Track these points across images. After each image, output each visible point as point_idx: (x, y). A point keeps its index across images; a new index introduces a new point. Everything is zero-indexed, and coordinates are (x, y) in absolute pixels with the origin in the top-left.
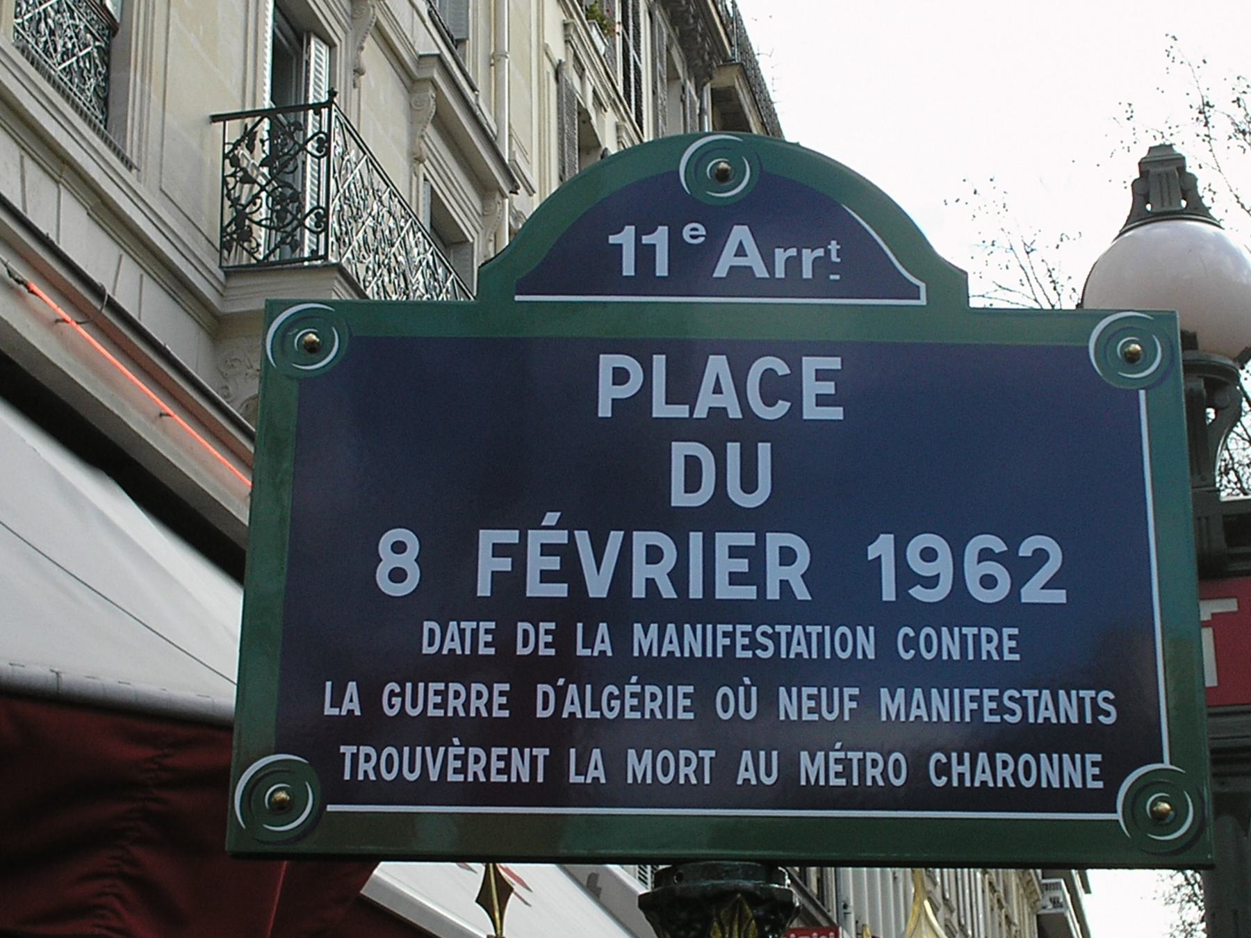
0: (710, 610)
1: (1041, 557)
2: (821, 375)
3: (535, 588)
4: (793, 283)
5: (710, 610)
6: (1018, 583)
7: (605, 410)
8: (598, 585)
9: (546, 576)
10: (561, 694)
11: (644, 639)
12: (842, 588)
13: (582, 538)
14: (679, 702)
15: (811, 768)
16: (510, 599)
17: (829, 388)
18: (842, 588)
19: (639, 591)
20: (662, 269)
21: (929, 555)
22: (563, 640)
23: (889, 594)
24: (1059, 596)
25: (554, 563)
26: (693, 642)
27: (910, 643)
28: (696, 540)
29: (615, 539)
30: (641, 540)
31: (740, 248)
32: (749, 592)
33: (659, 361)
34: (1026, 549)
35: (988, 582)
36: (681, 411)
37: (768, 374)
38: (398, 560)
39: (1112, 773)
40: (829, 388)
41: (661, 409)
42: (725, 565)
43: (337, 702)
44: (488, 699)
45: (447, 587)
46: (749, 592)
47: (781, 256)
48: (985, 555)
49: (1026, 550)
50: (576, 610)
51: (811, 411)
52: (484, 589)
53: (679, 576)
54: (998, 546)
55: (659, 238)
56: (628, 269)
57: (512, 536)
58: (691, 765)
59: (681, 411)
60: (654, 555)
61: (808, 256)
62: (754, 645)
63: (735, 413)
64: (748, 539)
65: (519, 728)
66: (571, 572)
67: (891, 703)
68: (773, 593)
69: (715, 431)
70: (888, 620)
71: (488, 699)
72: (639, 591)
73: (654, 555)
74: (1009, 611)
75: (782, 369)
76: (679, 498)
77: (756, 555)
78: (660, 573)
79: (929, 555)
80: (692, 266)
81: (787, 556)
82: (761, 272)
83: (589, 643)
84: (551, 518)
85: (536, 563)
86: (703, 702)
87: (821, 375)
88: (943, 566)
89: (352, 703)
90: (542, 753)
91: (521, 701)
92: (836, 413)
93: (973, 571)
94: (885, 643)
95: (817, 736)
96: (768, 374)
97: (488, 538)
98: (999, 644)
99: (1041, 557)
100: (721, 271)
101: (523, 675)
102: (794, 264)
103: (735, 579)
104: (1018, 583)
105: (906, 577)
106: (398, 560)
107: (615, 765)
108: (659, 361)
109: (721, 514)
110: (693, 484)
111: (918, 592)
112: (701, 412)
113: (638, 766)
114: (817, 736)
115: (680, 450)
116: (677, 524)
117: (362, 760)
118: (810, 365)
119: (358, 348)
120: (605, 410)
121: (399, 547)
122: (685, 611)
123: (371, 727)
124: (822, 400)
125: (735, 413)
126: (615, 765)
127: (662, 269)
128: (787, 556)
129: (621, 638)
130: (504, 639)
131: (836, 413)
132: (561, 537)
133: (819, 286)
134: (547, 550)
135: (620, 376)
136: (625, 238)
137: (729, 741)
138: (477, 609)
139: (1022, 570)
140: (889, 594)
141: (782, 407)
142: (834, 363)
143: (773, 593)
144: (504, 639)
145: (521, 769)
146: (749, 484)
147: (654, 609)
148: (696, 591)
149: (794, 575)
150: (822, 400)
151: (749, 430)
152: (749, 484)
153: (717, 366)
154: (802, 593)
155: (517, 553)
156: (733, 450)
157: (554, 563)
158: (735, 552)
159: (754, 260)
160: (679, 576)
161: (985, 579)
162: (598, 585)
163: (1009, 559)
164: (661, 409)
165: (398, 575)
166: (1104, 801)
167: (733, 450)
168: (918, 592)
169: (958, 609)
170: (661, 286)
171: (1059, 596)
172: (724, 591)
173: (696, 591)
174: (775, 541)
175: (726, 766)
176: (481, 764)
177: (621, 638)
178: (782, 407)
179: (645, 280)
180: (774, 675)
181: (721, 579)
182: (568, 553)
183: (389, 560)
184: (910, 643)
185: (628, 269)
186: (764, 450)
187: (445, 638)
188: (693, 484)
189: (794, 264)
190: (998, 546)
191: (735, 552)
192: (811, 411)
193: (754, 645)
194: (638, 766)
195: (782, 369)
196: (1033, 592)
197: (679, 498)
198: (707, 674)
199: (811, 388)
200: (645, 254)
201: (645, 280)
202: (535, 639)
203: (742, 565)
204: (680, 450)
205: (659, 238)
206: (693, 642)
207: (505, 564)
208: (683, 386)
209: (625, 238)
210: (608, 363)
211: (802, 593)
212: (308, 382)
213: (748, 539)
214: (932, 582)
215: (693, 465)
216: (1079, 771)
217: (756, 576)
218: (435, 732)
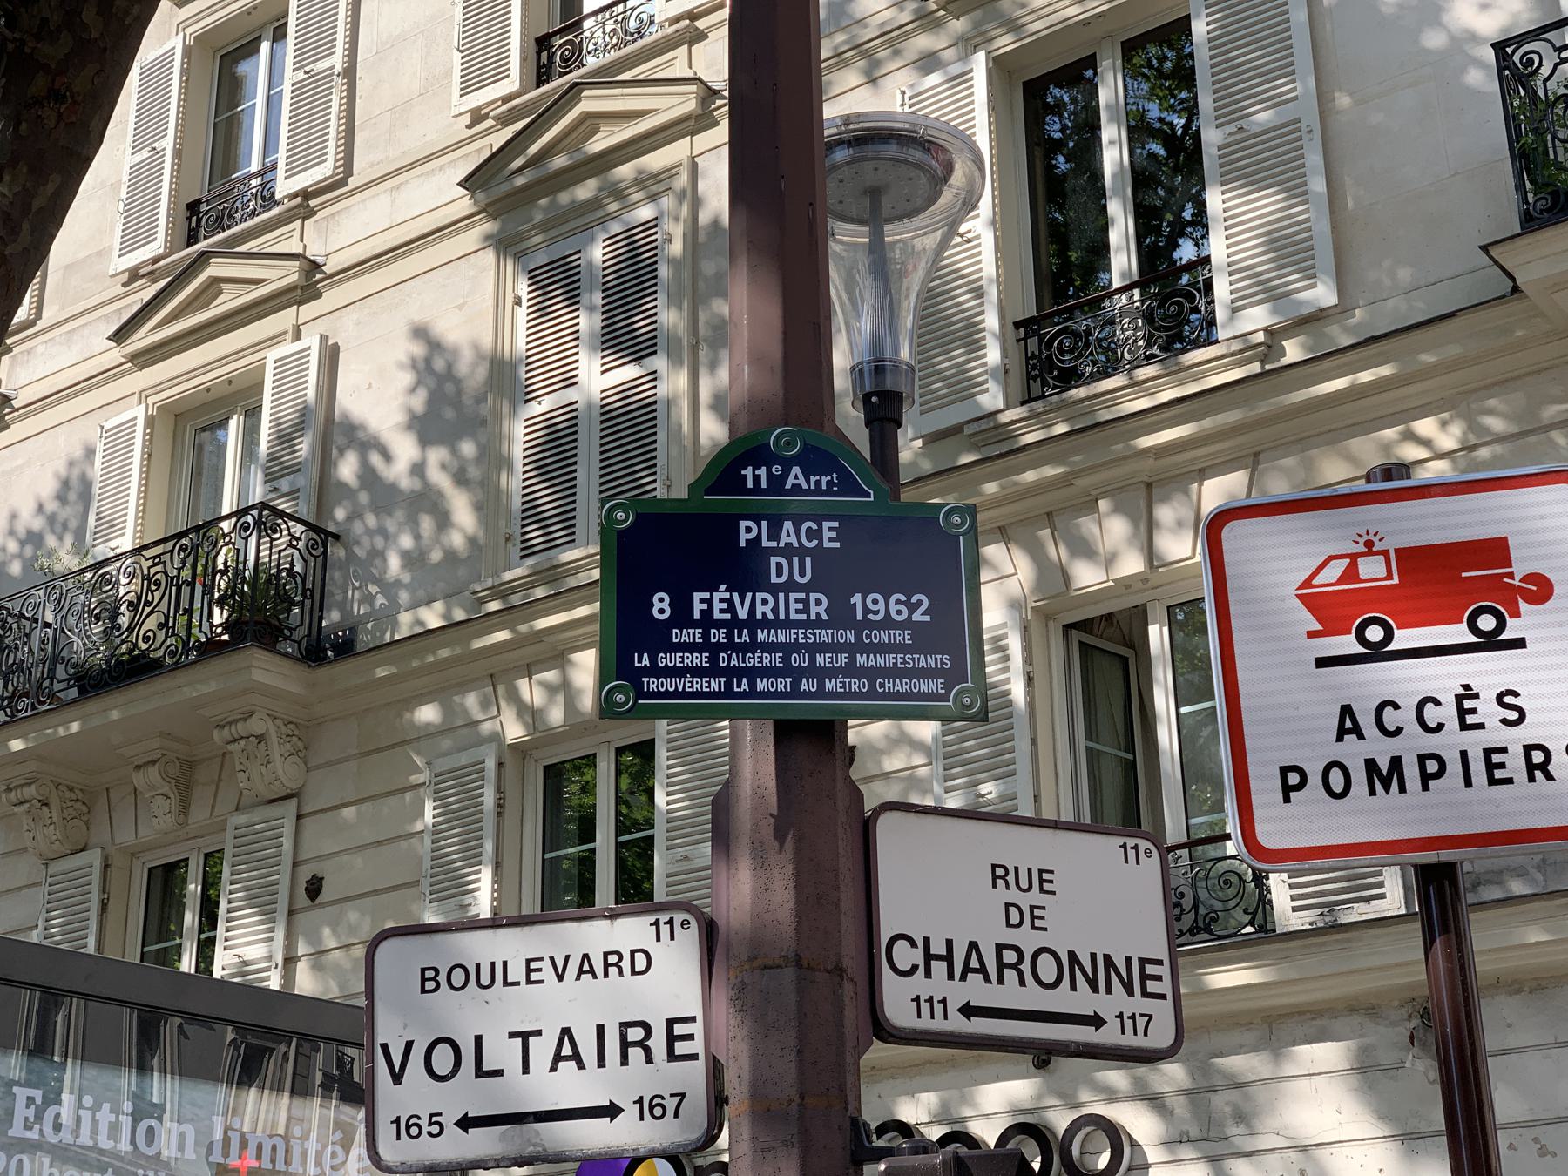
0: (788, 624)
1: (920, 602)
2: (831, 529)
3: (717, 616)
4: (818, 491)
5: (788, 624)
6: (911, 613)
7: (742, 544)
8: (743, 614)
9: (722, 611)
10: (730, 657)
11: (762, 635)
12: (841, 616)
13: (736, 595)
14: (777, 660)
15: (830, 685)
16: (707, 620)
17: (834, 534)
18: (841, 616)
19: (759, 617)
20: (764, 485)
21: (875, 602)
22: (729, 636)
23: (860, 617)
24: (927, 618)
25: (724, 606)
26: (782, 636)
27: (868, 636)
28: (781, 596)
29: (749, 596)
30: (760, 596)
31: (796, 476)
32: (804, 617)
33: (764, 523)
34: (914, 599)
35: (899, 612)
36: (774, 544)
37: (809, 528)
38: (661, 605)
39: (948, 687)
40: (834, 534)
41: (765, 543)
42: (793, 606)
43: (640, 661)
44: (701, 660)
45: (682, 615)
46: (804, 617)
47: (813, 479)
48: (898, 602)
49: (914, 599)
50: (734, 624)
51: (827, 544)
52: (697, 616)
53: (775, 610)
54: (903, 598)
55: (762, 472)
56: (750, 485)
57: (707, 595)
58: (781, 684)
59: (774, 544)
60: (765, 602)
61: (824, 480)
62: (806, 637)
63: (796, 545)
64: (803, 596)
65: (713, 671)
66: (731, 608)
67: (861, 660)
68: (813, 617)
69: (788, 552)
70: (859, 627)
71: (701, 660)
72: (759, 617)
73: (765, 602)
74: (907, 624)
75: (815, 527)
76: (774, 579)
77: (806, 602)
78: (768, 609)
79: (875, 602)
80: (777, 484)
81: (818, 603)
82: (805, 486)
83: (740, 637)
84: (723, 588)
85: (717, 606)
86: (786, 660)
87: (831, 529)
88: (881, 606)
89: (646, 661)
90: (723, 680)
91: (714, 660)
92: (837, 545)
93: (893, 609)
94: (858, 636)
95: (832, 673)
96: (809, 528)
97: (697, 596)
98: (903, 637)
99: (920, 602)
100: (788, 486)
101: (714, 650)
102: (818, 483)
103: (798, 611)
104: (911, 613)
105: (866, 610)
106: (661, 605)
107: (752, 684)
108: (764, 523)
109: (790, 586)
110: (779, 574)
111: (871, 616)
112: (782, 545)
113: (761, 684)
114: (832, 673)
115: (774, 560)
116: (774, 590)
117: (651, 684)
118: (826, 525)
119: (640, 518)
120: (742, 544)
121: (661, 600)
122: (776, 624)
123: (654, 671)
124: (831, 540)
125: (796, 545)
126: (752, 684)
127: (764, 485)
128: (818, 603)
129: (753, 635)
130: (706, 635)
131: (837, 545)
132: (727, 595)
133: (829, 492)
134: (721, 600)
135: (748, 530)
136: (748, 472)
137: (797, 674)
138: (695, 624)
139: (912, 608)
140: (860, 617)
141: (815, 542)
142: (836, 524)
143: (813, 617)
144: (706, 635)
145: (715, 686)
146: (802, 574)
147: (765, 624)
148: (782, 617)
149: (822, 610)
150: (831, 540)
151: (802, 552)
152: (802, 574)
153: (788, 525)
154: (825, 617)
155: (710, 601)
156: (796, 559)
157: (724, 606)
158: (797, 601)
159: (802, 481)
160: (775, 610)
161: (899, 612)
162: (743, 614)
163: (907, 603)
164: (765, 543)
165: (661, 611)
166: (945, 698)
167: (796, 559)
168: (871, 616)
169: (888, 623)
170: (763, 492)
171: (927, 618)
172: (793, 616)
173: (782, 617)
174: (813, 596)
175: (796, 684)
176: (699, 684)
177: (753, 635)
178: (815, 542)
179: (757, 490)
180: (815, 649)
181: (792, 611)
182: (730, 601)
183: (657, 606)
184: (868, 636)
185: (750, 485)
186: (808, 559)
187: (681, 636)
188: (779, 574)
189: (818, 483)
190: (903, 598)
191: (797, 601)
192: (827, 544)
193: (806, 637)
194: (761, 684)
195: (815, 527)
196: (917, 617)
197: (774, 579)
198: (787, 649)
199: (827, 534)
200: (757, 479)
201: (757, 490)
202: (718, 636)
203: (800, 606)
204: (774, 560)
205: (762, 472)
206: (782, 636)
207: (705, 606)
208: (774, 535)
209: (748, 472)
210: (743, 524)
211: (825, 617)
212: (621, 533)
213: (803, 596)
214: (876, 612)
215: (779, 565)
216: (935, 686)
217: (806, 610)
218: (679, 672)
